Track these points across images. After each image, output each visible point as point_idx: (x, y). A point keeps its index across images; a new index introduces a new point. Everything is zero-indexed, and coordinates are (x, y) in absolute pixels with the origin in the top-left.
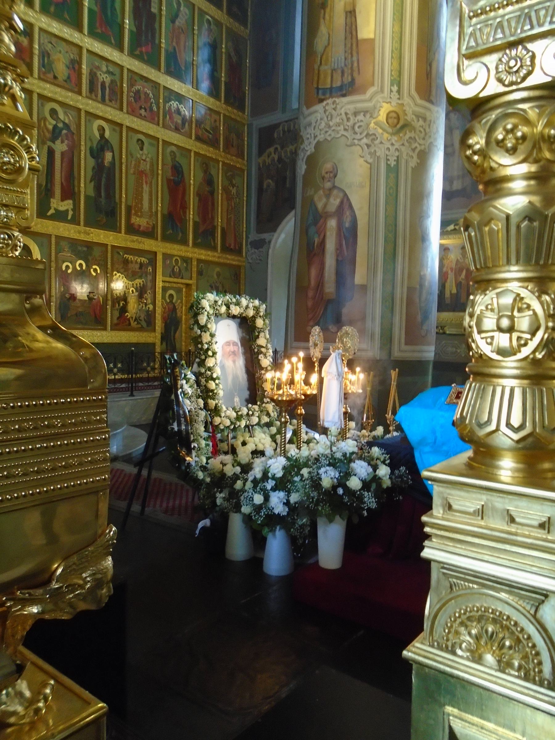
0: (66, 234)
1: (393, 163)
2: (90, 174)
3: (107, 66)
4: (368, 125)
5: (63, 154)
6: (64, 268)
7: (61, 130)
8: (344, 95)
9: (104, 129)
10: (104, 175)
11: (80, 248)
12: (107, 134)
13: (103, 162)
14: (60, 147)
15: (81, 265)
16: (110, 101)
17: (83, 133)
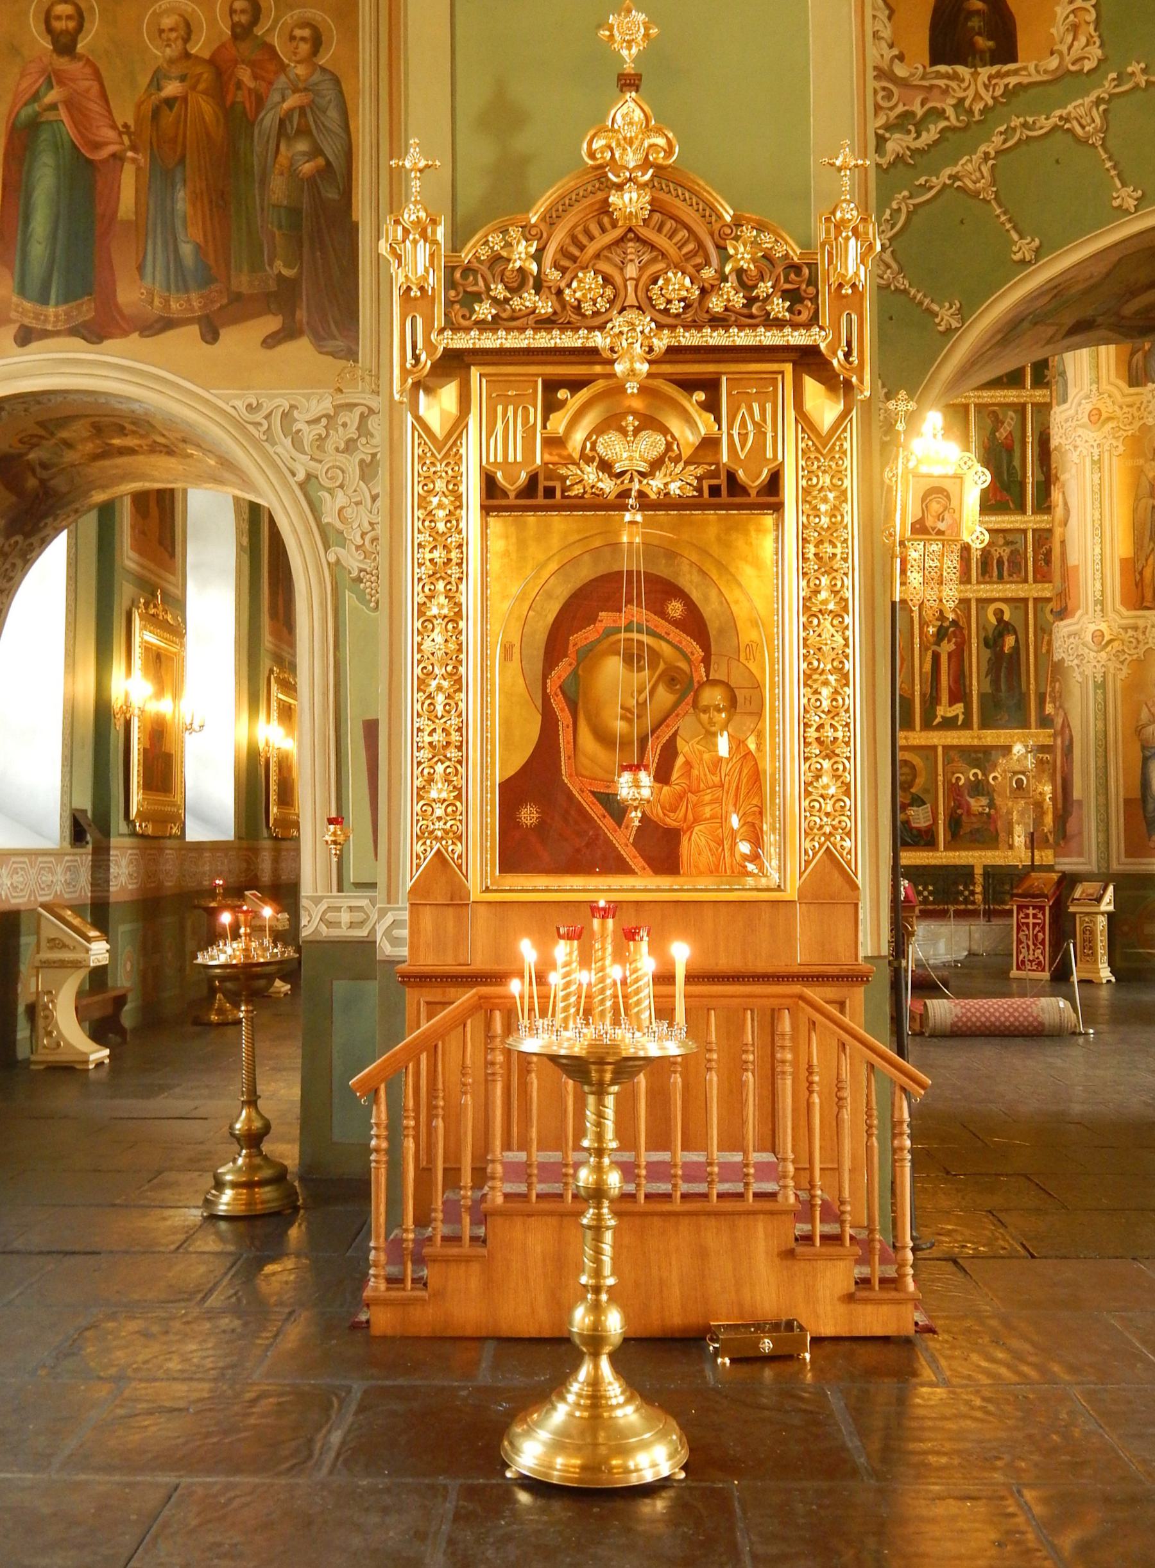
0: (955, 742)
1: (1100, 680)
2: (985, 666)
3: (1005, 538)
4: (1077, 646)
5: (950, 655)
6: (954, 781)
7: (948, 628)
8: (1062, 620)
9: (1002, 612)
10: (1005, 665)
11: (973, 755)
12: (1006, 617)
13: (1002, 650)
14: (947, 647)
15: (975, 775)
16: (1010, 575)
17: (974, 626)
